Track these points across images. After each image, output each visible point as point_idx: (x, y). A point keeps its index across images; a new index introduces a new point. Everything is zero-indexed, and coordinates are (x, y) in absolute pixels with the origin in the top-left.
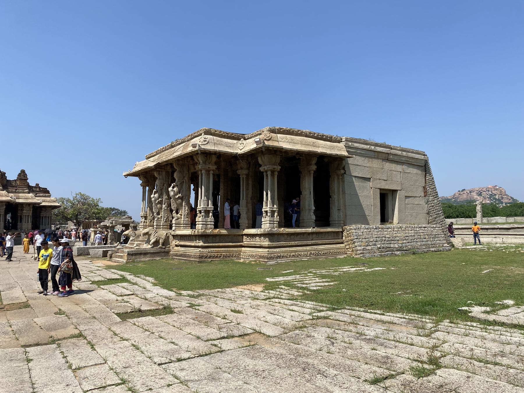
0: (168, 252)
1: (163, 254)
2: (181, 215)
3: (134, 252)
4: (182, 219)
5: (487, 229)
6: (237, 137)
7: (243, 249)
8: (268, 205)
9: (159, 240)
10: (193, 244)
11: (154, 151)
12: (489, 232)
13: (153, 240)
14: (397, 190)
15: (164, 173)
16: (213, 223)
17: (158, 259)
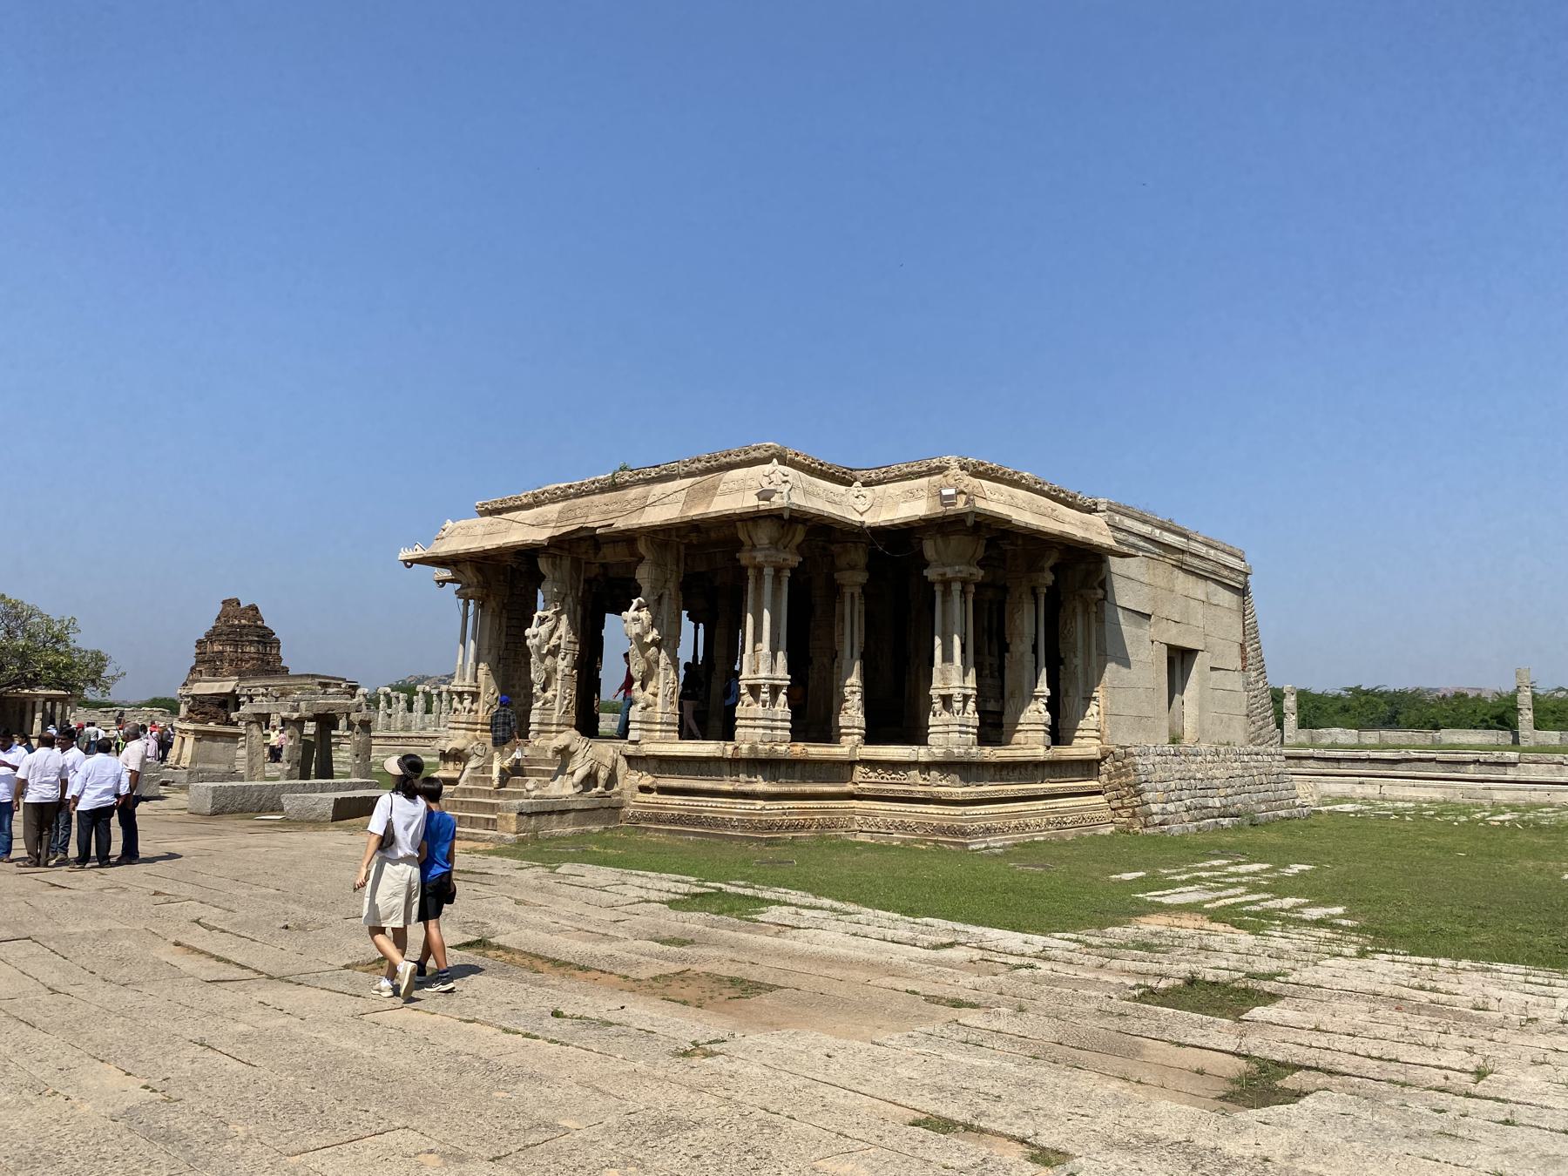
0: (617, 808)
1: (606, 814)
2: (655, 695)
3: (535, 809)
4: (659, 709)
5: (1338, 760)
6: (843, 479)
7: (854, 803)
8: (952, 676)
9: (597, 772)
10: (726, 786)
11: (525, 496)
12: (1344, 768)
13: (580, 773)
14: (1196, 651)
15: (567, 563)
16: (788, 725)
17: (596, 828)
